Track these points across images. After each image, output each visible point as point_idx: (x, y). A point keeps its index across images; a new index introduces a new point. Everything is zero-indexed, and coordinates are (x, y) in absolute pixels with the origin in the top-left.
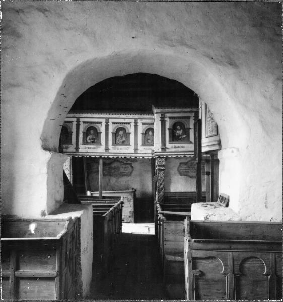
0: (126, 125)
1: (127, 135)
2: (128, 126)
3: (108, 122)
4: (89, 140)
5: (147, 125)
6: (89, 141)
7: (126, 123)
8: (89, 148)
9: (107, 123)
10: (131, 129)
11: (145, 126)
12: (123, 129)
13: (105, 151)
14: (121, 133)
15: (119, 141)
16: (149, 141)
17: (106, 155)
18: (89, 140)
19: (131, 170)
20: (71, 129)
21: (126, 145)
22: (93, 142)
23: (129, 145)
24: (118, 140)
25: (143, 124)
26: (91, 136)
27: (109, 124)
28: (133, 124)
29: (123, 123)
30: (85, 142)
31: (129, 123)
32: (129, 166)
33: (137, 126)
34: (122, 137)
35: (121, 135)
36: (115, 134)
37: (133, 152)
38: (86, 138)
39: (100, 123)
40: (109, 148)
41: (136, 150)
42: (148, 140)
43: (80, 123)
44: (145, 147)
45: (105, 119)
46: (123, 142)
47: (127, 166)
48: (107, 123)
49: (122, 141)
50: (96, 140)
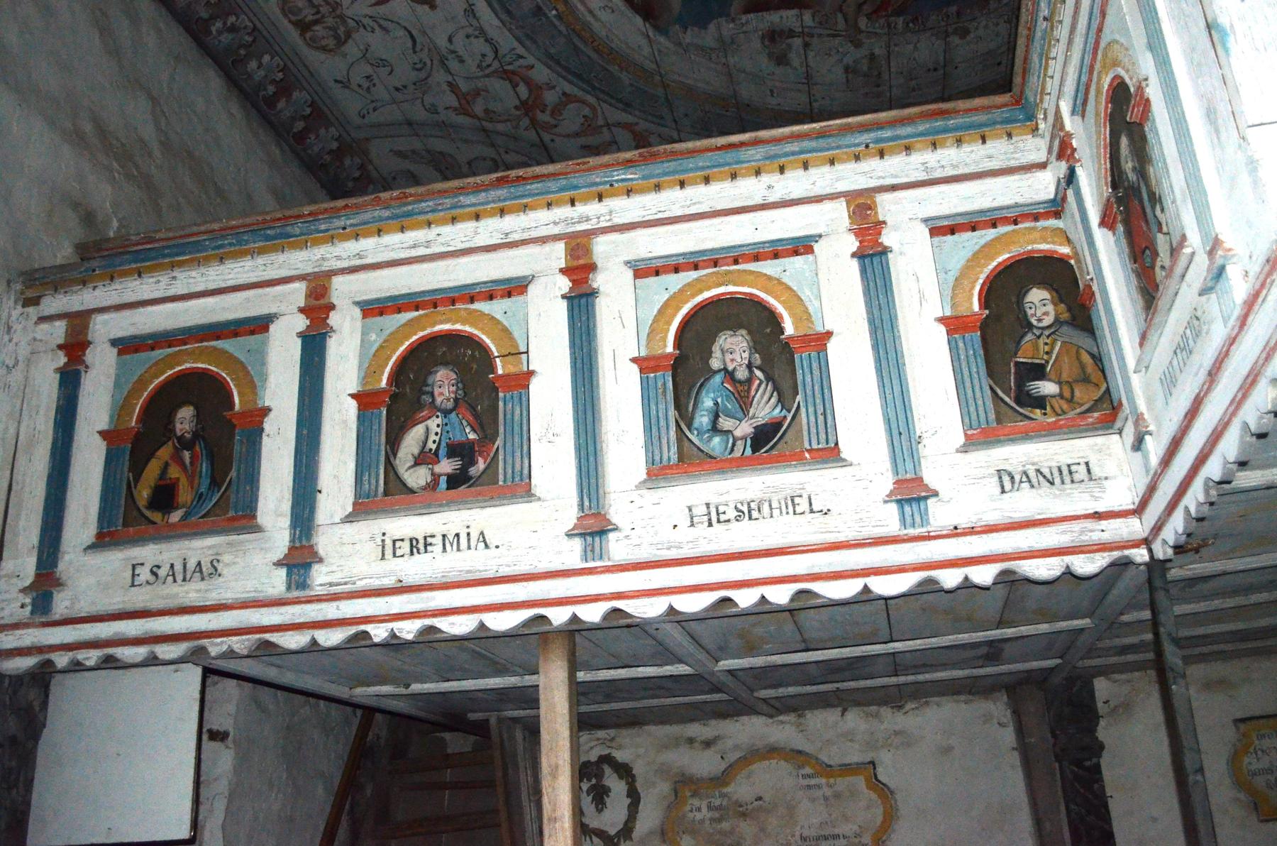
0: (769, 268)
1: (786, 356)
2: (791, 269)
3: (592, 267)
4: (423, 458)
5: (991, 234)
6: (417, 478)
7: (759, 253)
8: (417, 546)
9: (580, 272)
10: (828, 293)
11: (969, 242)
12: (755, 318)
13: (572, 554)
14: (733, 350)
15: (715, 429)
16: (1047, 388)
17: (587, 600)
18: (423, 458)
19: (878, 814)
20: (252, 385)
21: (795, 458)
22: (455, 481)
23: (830, 454)
24: (703, 420)
25: (942, 228)
26: (434, 423)
27: (599, 281)
28: (839, 247)
29: (739, 255)
30: (382, 492)
31: (802, 247)
32: (860, 782)
33: (885, 251)
34: (742, 396)
35: (730, 375)
36: (681, 370)
37: (889, 520)
38: (393, 443)
39: (515, 288)
40: (617, 510)
41: (911, 493)
42: (1038, 372)
43: (334, 319)
44: (1017, 455)
45: (560, 248)
46: (764, 437)
47: (842, 783)
48: (580, 272)
49: (744, 429)
50: (480, 463)
